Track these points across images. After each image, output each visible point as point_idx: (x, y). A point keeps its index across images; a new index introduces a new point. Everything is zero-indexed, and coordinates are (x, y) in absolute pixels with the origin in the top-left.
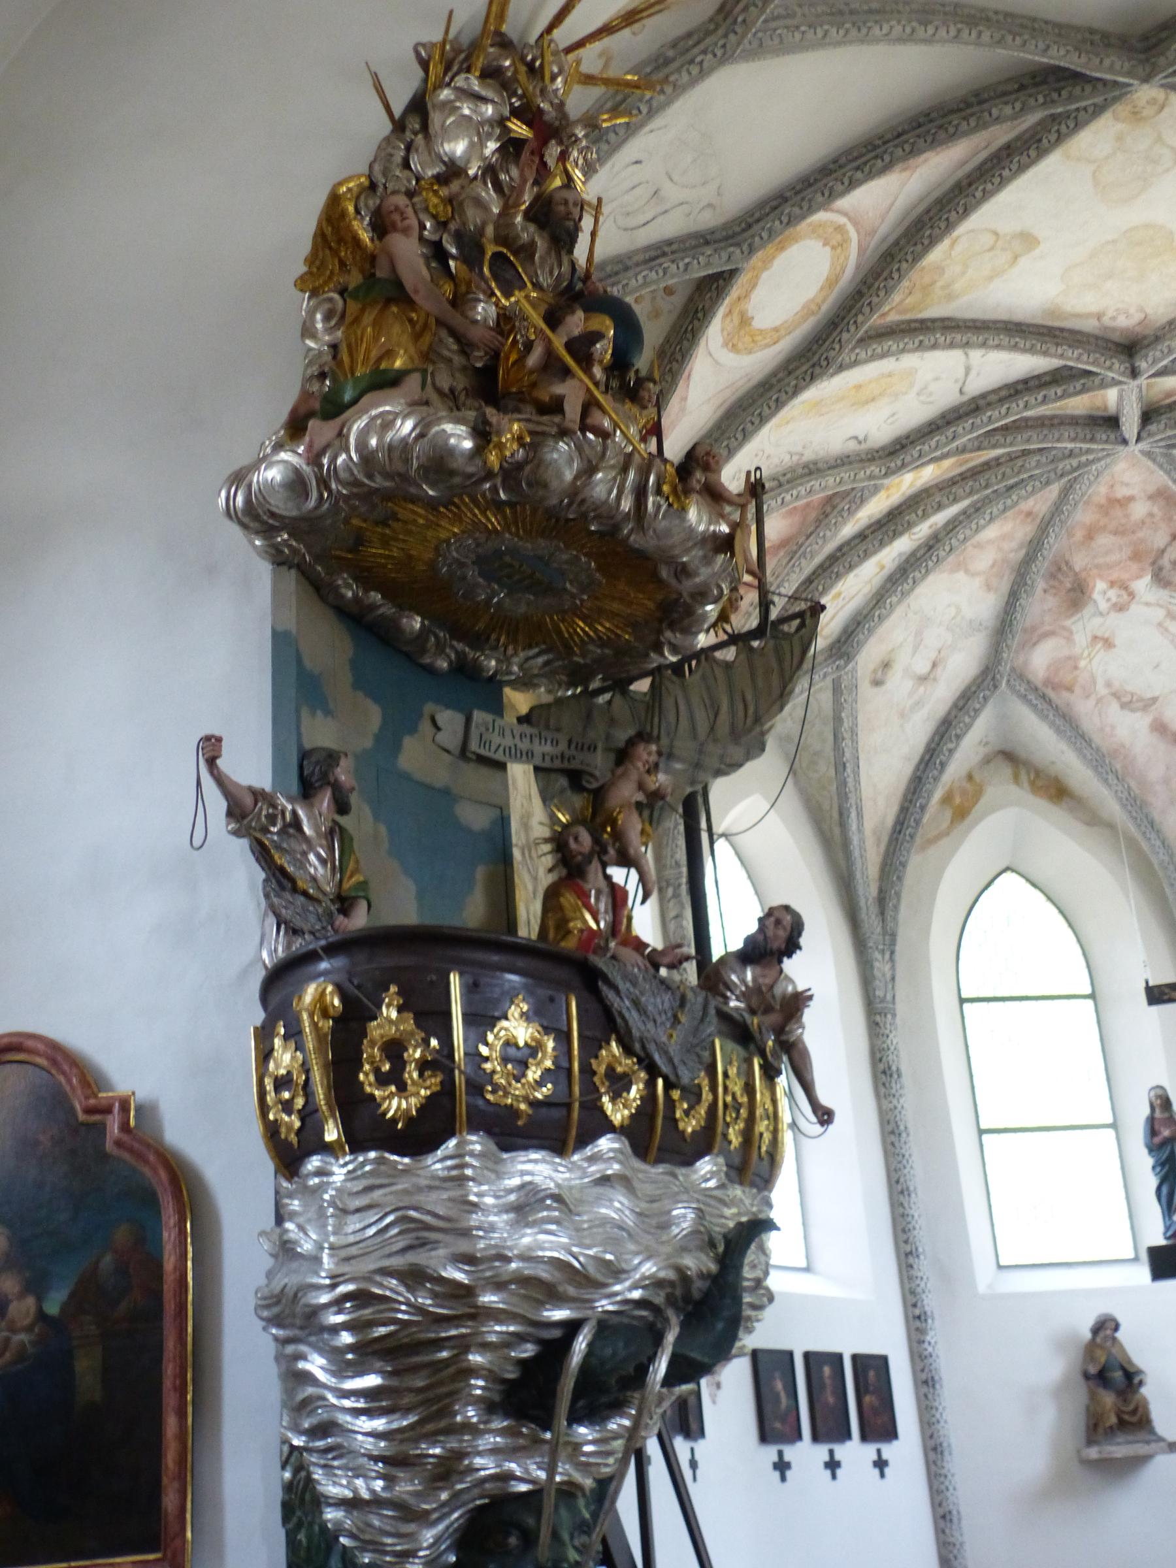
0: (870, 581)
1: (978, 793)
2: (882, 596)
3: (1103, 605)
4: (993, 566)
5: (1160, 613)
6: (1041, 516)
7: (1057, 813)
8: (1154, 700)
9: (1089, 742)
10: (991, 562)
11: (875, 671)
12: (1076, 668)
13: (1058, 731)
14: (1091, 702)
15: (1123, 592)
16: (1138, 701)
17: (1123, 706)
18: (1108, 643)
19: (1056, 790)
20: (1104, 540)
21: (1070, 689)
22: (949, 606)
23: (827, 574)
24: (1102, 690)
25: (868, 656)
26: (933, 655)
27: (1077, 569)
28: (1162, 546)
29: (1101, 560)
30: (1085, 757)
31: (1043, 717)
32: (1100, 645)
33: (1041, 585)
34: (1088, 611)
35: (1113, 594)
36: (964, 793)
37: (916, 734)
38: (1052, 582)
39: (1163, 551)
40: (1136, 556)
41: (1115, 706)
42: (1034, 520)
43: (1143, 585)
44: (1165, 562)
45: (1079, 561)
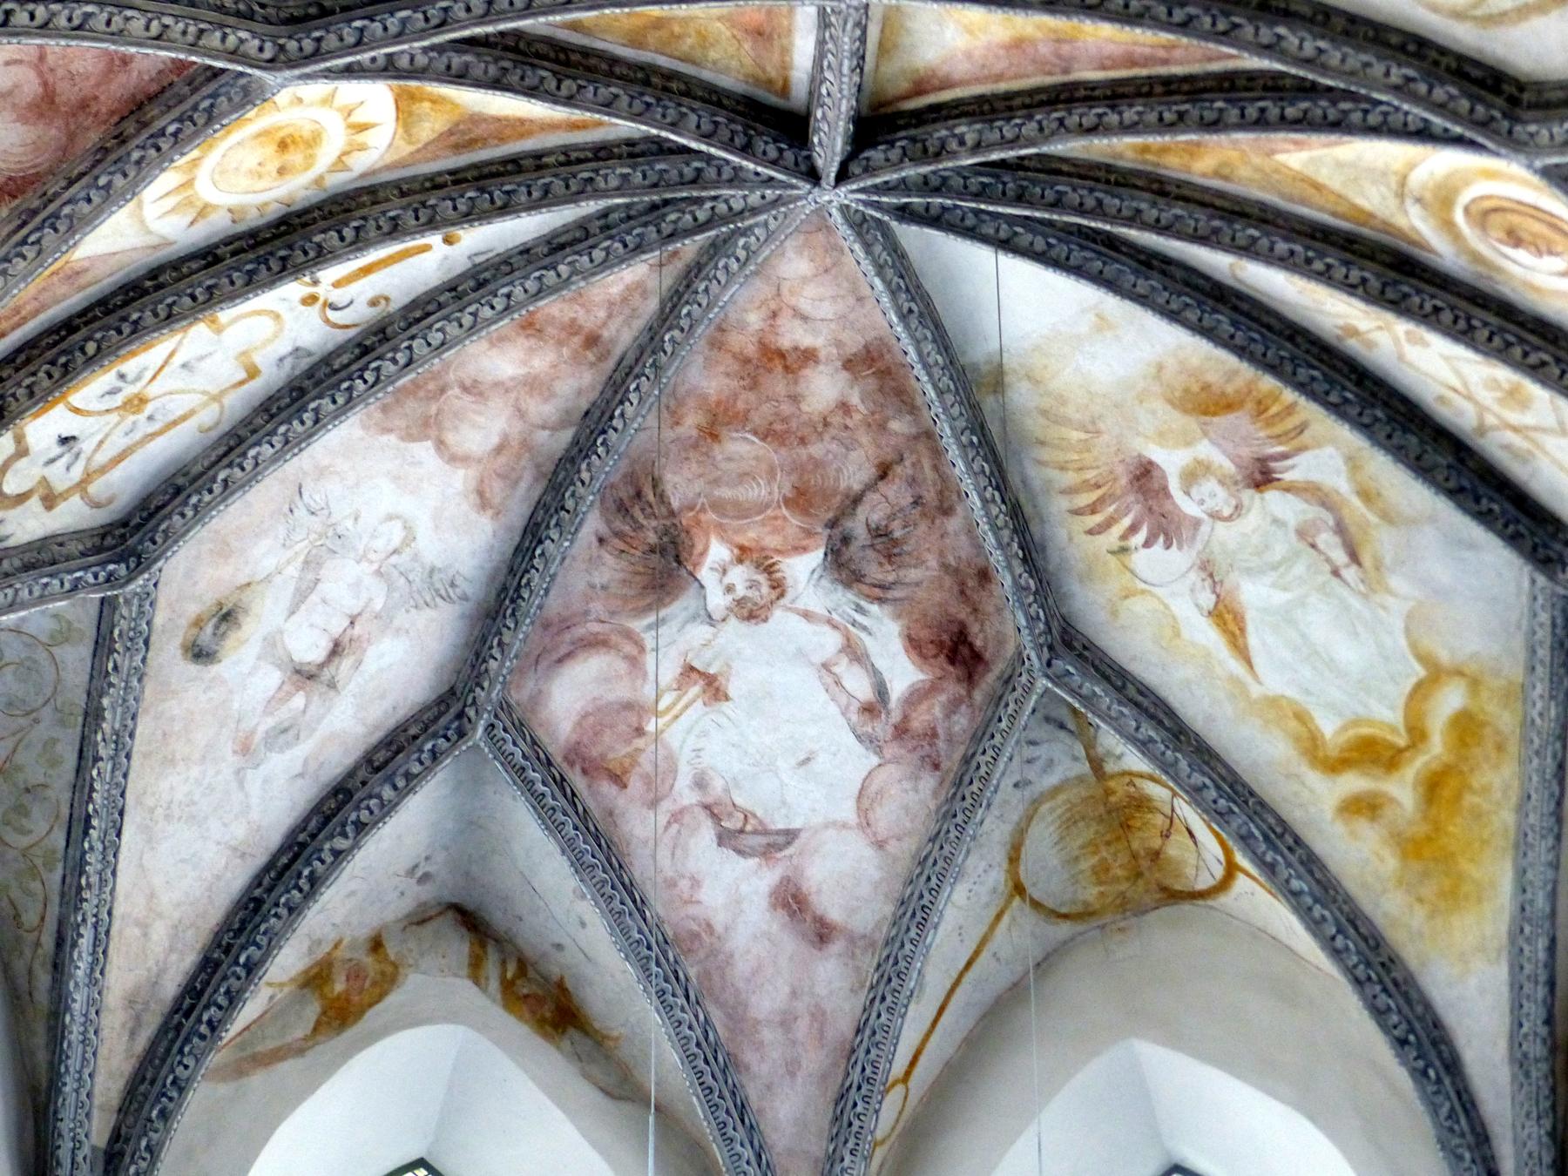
0: (216, 398)
2: (241, 440)
3: (717, 600)
4: (499, 450)
5: (830, 641)
6: (617, 352)
7: (550, 1057)
8: (790, 835)
9: (640, 905)
10: (495, 440)
11: (198, 623)
12: (639, 731)
15: (761, 578)
16: (755, 832)
17: (726, 838)
18: (714, 689)
19: (555, 1010)
20: (740, 447)
21: (619, 780)
22: (390, 518)
23: (112, 320)
25: (188, 574)
26: (337, 626)
27: (675, 504)
28: (857, 487)
29: (725, 493)
30: (625, 933)
31: (554, 827)
32: (695, 690)
33: (593, 524)
34: (678, 609)
35: (740, 576)
36: (355, 974)
37: (272, 800)
38: (619, 524)
39: (856, 500)
40: (800, 500)
42: (602, 358)
43: (803, 568)
44: (857, 526)
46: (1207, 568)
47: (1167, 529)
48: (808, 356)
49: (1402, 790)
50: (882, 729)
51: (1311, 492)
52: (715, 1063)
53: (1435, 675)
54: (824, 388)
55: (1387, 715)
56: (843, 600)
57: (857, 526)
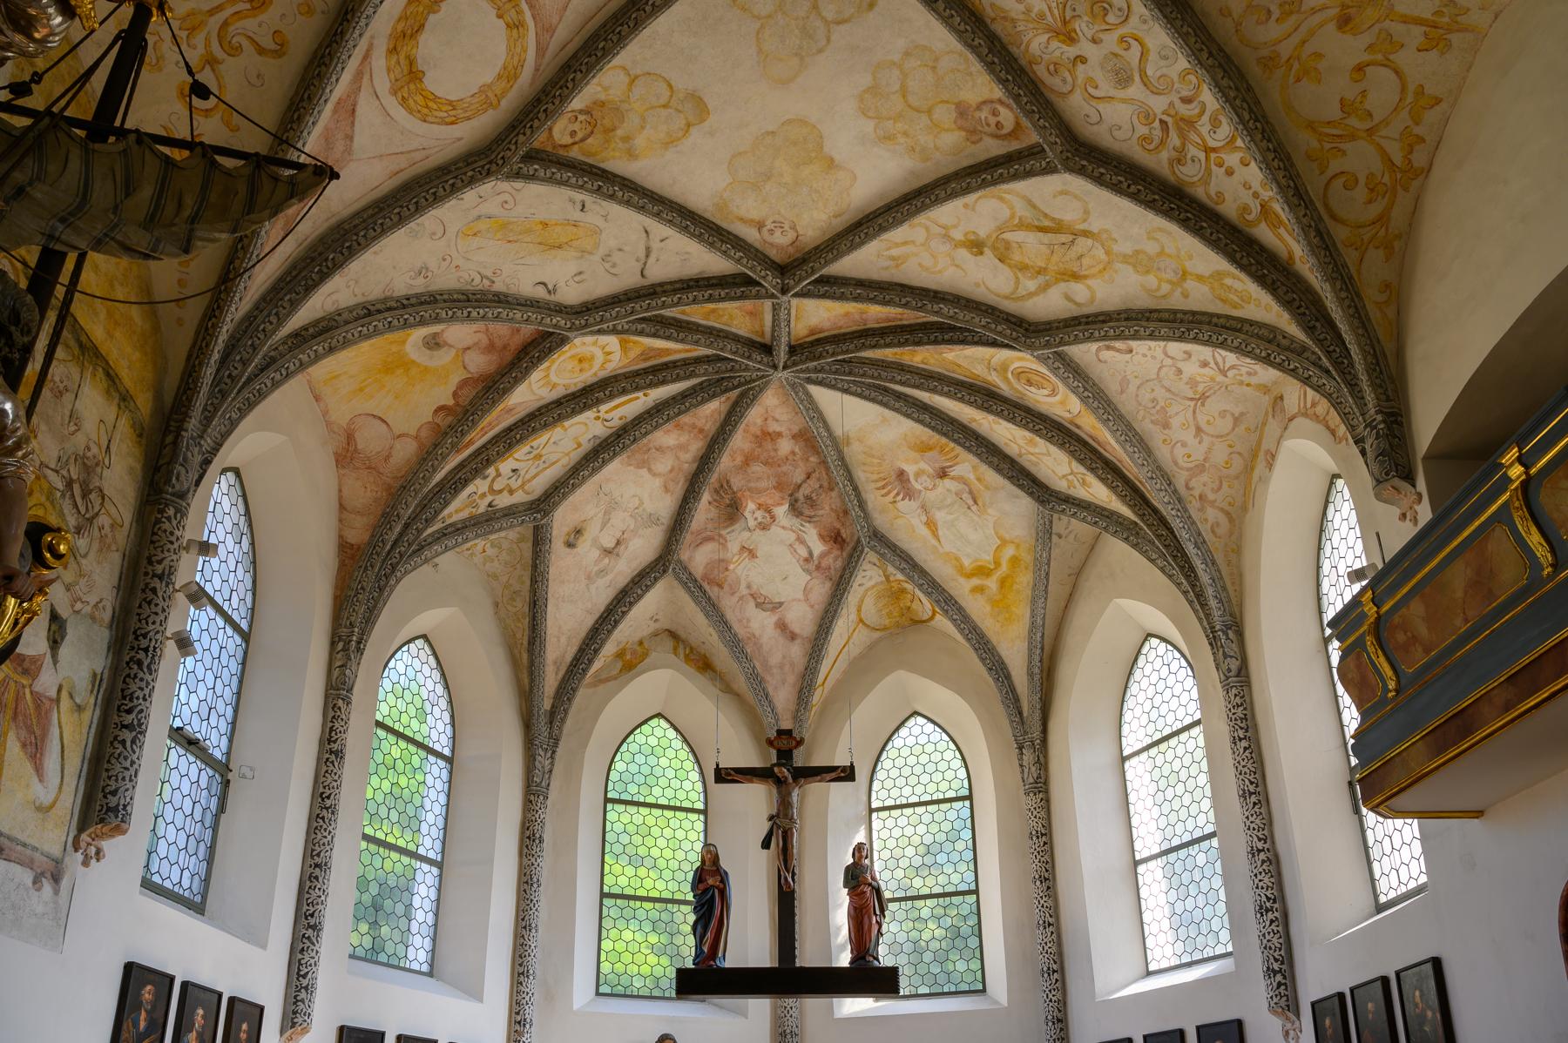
1: (645, 655)
3: (752, 523)
5: (793, 536)
8: (781, 604)
9: (730, 629)
13: (707, 615)
14: (735, 599)
17: (758, 605)
18: (752, 554)
20: (757, 468)
21: (720, 586)
24: (743, 591)
31: (698, 603)
33: (706, 497)
35: (759, 514)
41: (752, 604)
43: (781, 511)
44: (800, 495)
45: (737, 482)
46: (923, 507)
47: (909, 494)
48: (779, 434)
49: (992, 584)
50: (812, 567)
51: (961, 479)
52: (756, 680)
53: (1004, 542)
54: (785, 446)
55: (987, 558)
56: (796, 522)
57: (800, 495)
